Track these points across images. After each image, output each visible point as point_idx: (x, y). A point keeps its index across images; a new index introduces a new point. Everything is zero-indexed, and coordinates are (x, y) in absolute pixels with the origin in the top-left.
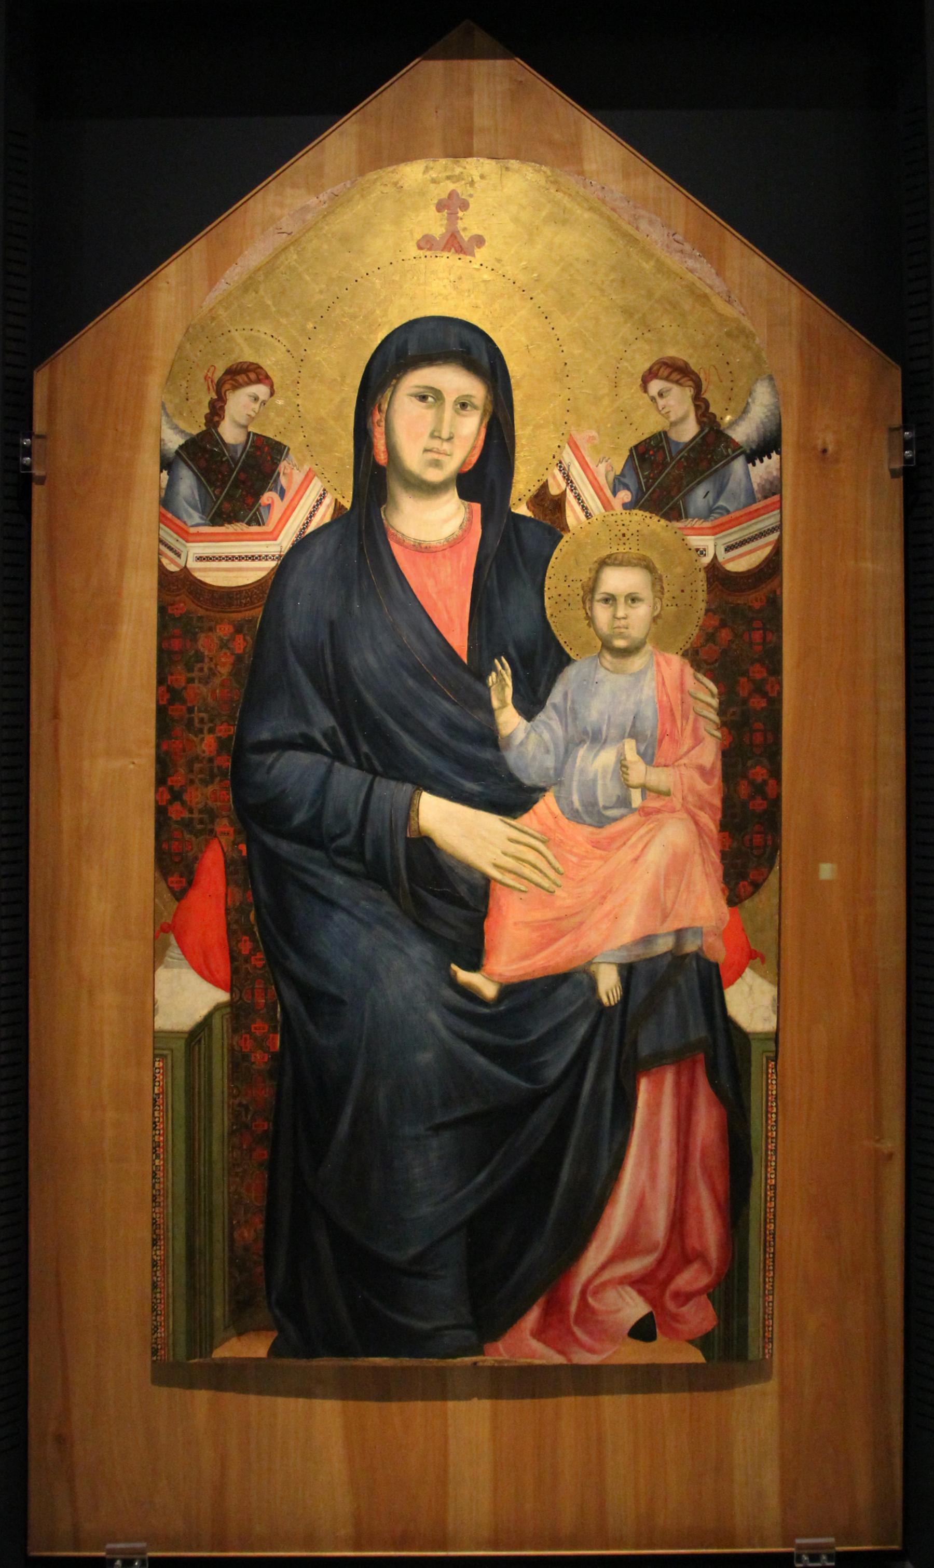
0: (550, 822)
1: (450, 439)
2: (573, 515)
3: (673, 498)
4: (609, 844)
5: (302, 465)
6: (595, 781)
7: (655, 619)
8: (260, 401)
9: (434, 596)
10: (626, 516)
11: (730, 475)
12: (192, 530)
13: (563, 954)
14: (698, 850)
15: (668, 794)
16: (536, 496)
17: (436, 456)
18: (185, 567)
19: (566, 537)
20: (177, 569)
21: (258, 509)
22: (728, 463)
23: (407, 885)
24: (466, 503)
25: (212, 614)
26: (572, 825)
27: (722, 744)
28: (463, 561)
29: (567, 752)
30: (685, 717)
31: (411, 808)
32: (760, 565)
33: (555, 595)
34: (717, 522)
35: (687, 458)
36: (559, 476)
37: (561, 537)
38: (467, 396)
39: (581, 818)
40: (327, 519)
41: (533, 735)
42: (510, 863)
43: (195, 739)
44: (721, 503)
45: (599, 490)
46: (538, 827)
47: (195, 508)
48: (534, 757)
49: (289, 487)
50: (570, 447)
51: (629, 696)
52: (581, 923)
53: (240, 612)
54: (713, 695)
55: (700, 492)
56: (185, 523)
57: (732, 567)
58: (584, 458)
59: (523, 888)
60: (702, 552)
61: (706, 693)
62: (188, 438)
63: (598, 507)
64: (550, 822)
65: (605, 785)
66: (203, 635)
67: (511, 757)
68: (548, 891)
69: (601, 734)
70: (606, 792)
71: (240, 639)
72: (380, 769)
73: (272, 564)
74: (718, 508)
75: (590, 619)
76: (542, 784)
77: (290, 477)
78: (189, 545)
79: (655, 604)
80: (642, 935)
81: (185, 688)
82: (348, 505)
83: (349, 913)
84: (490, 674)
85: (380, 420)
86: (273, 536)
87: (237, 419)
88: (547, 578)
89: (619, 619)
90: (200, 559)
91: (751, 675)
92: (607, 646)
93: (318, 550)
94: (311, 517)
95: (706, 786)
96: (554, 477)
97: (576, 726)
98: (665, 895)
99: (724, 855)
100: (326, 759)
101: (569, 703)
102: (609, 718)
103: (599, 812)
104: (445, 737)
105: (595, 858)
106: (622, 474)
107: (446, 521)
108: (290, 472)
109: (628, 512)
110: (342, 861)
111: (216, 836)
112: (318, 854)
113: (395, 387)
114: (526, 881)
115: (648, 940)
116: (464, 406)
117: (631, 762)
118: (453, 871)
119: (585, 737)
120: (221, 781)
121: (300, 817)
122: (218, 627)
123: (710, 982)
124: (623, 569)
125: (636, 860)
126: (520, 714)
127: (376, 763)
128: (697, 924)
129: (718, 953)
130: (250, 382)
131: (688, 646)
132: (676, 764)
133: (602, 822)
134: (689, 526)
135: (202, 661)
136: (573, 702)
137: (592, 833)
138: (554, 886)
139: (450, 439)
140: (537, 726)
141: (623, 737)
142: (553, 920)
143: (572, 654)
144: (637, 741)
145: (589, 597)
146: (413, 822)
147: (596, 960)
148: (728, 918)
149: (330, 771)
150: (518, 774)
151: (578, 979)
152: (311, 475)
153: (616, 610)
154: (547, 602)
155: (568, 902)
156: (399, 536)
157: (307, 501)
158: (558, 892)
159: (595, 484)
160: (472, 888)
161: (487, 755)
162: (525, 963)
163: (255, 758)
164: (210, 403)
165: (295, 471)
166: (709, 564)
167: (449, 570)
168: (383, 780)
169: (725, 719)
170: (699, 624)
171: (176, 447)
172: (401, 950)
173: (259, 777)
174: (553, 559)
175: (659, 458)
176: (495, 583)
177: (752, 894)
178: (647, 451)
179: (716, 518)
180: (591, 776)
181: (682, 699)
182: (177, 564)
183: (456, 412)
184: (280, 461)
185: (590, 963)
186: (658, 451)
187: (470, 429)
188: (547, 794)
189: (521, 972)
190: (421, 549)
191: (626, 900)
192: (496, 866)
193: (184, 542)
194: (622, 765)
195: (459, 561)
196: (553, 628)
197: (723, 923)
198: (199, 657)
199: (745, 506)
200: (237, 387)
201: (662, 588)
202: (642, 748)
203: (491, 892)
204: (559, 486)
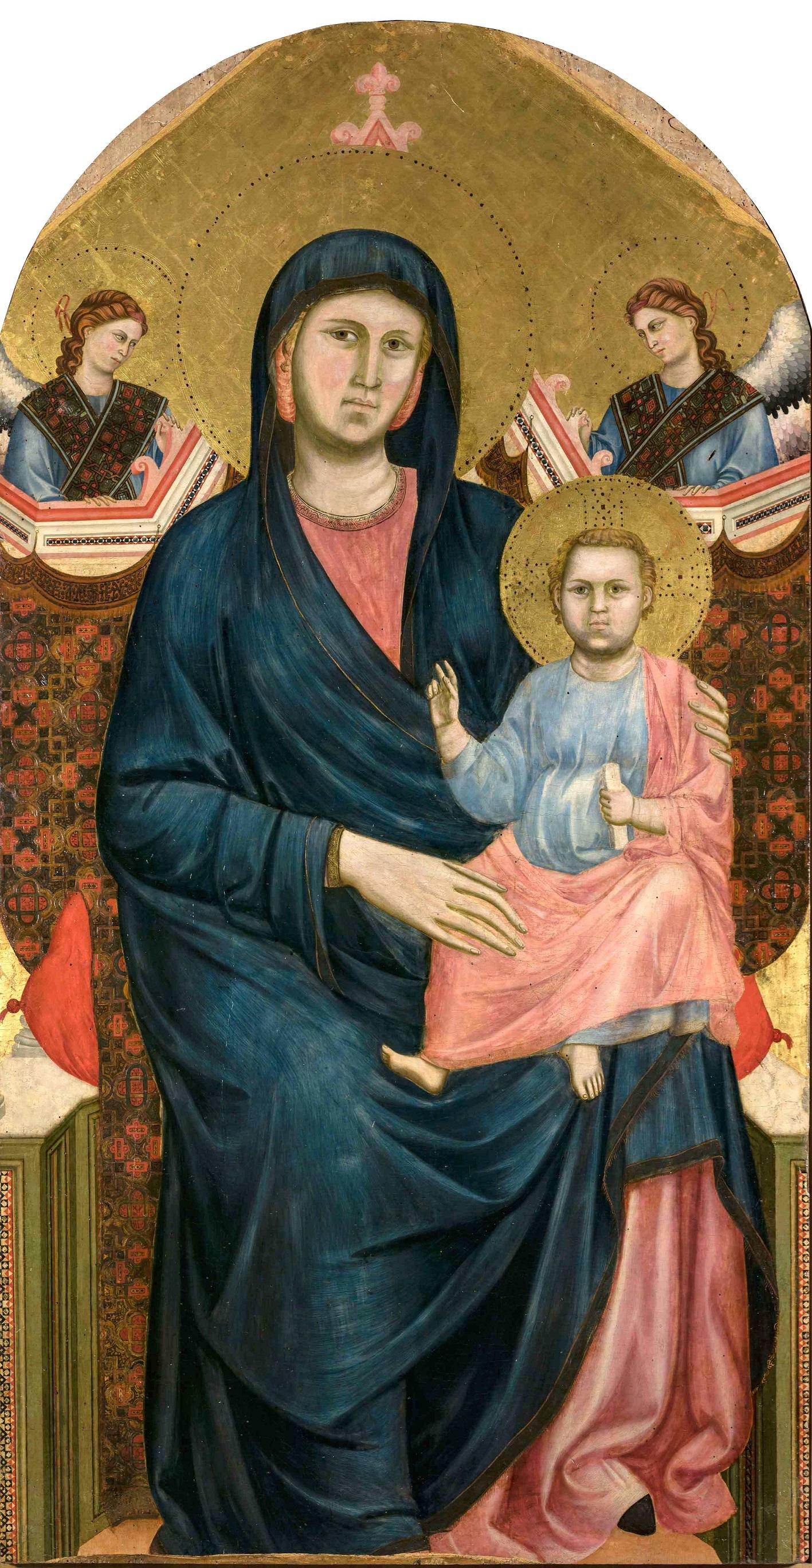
0: (508, 867)
1: (376, 387)
3: (669, 459)
4: (586, 895)
5: (185, 419)
6: (567, 815)
7: (645, 613)
8: (129, 341)
9: (357, 585)
11: (744, 429)
12: (42, 506)
13: (528, 1033)
14: (702, 903)
15: (662, 832)
16: (488, 458)
17: (358, 409)
18: (34, 552)
19: (527, 510)
21: (127, 479)
22: (741, 414)
23: (324, 947)
24: (398, 467)
25: (70, 612)
26: (537, 870)
27: (733, 770)
29: (530, 778)
30: (684, 735)
31: (329, 850)
32: (782, 544)
34: (726, 490)
35: (687, 409)
36: (519, 434)
37: (522, 509)
38: (398, 331)
39: (548, 861)
40: (218, 491)
41: (486, 758)
42: (458, 919)
43: (49, 768)
44: (731, 465)
45: (569, 449)
46: (493, 873)
47: (46, 479)
48: (488, 786)
49: (168, 450)
50: (533, 396)
51: (610, 710)
52: (552, 994)
53: (107, 608)
54: (721, 709)
55: (704, 450)
56: (32, 496)
57: (744, 546)
58: (550, 409)
59: (475, 950)
60: (706, 528)
61: (712, 706)
62: (35, 388)
63: (569, 472)
64: (508, 867)
65: (579, 820)
66: (58, 638)
67: (458, 787)
68: (506, 953)
69: (575, 758)
70: (581, 829)
71: (106, 641)
72: (289, 802)
73: (148, 547)
74: (725, 472)
75: (560, 614)
76: (498, 820)
77: (168, 437)
78: (37, 524)
79: (644, 593)
80: (630, 1010)
81: (34, 705)
82: (244, 472)
83: (251, 983)
84: (429, 682)
85: (285, 364)
86: (148, 512)
87: (100, 363)
88: (503, 561)
89: (597, 613)
90: (52, 542)
91: (771, 681)
92: (581, 647)
94: (196, 487)
95: (712, 823)
96: (512, 434)
97: (541, 748)
98: (659, 961)
99: (736, 910)
100: (219, 791)
101: (533, 719)
102: (585, 736)
103: (572, 854)
104: (371, 761)
105: (569, 913)
106: (601, 430)
107: (372, 491)
108: (169, 432)
109: (608, 477)
110: (239, 918)
111: (78, 890)
112: (209, 909)
113: (304, 320)
114: (477, 941)
115: (638, 1015)
116: (394, 344)
117: (614, 792)
118: (385, 929)
119: (553, 761)
120: (84, 820)
121: (187, 864)
122: (78, 628)
123: (720, 1071)
124: (602, 549)
125: (620, 915)
126: (469, 733)
127: (284, 795)
128: (702, 996)
129: (730, 1033)
130: (116, 317)
131: (689, 645)
132: (673, 794)
133: (575, 866)
134: (689, 494)
135: (57, 671)
136: (538, 718)
137: (564, 882)
138: (515, 948)
139: (376, 387)
140: (492, 748)
141: (604, 762)
142: (514, 989)
143: (536, 658)
144: (621, 766)
145: (559, 585)
146: (331, 868)
147: (571, 1041)
148: (742, 989)
149: (224, 806)
150: (466, 807)
151: (547, 1065)
152: (196, 434)
153: (592, 601)
154: (504, 594)
155: (533, 968)
156: (311, 510)
157: (193, 463)
158: (520, 955)
159: (566, 442)
160: (409, 950)
161: (428, 783)
162: (478, 1044)
163: (125, 791)
164: (63, 342)
165: (176, 430)
166: (715, 543)
167: (376, 554)
168: (294, 816)
169: (736, 738)
170: (703, 619)
171: (19, 400)
172: (319, 1029)
173: (133, 814)
174: (511, 538)
175: (650, 409)
176: (436, 568)
177: (776, 958)
178: (633, 400)
179: (724, 485)
180: (562, 809)
181: (680, 713)
182: (22, 550)
183: (384, 351)
185: (562, 1044)
186: (648, 400)
187: (402, 370)
188: (505, 831)
189: (473, 1056)
190: (339, 526)
191: (608, 965)
192: (440, 922)
193: (32, 522)
194: (602, 796)
196: (511, 624)
197: (735, 994)
198: (53, 666)
199: (763, 469)
201: (653, 573)
202: (628, 775)
203: (433, 954)
204: (519, 445)
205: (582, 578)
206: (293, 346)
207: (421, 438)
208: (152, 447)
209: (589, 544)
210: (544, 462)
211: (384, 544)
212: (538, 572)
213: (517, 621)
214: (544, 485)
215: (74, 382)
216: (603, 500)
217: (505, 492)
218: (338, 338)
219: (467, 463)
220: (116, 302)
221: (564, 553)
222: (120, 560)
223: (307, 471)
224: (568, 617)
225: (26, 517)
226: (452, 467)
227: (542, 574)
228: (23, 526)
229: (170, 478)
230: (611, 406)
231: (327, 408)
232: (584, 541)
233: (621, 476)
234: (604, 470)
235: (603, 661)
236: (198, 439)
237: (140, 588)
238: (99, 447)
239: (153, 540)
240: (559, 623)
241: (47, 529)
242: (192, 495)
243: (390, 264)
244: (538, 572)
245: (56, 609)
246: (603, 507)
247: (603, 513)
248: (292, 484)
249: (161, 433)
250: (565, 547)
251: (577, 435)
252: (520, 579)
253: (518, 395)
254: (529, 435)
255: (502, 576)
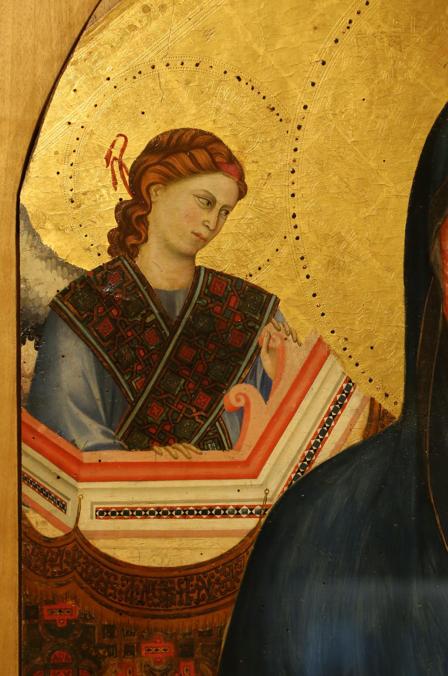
8: (218, 207)
12: (87, 458)
18: (76, 528)
20: (59, 533)
21: (218, 418)
25: (132, 621)
40: (356, 438)
47: (94, 415)
53: (188, 616)
56: (73, 443)
62: (76, 277)
77: (280, 356)
78: (81, 485)
86: (250, 469)
90: (104, 513)
93: (338, 497)
94: (323, 433)
122: (143, 646)
152: (322, 352)
164: (117, 209)
165: (290, 344)
171: (52, 295)
182: (58, 524)
184: (260, 323)
193: (72, 481)
200: (171, 178)
208: (254, 371)
215: (136, 269)
220: (198, 147)
222: (208, 542)
225: (63, 475)
228: (58, 488)
229: (283, 418)
236: (325, 358)
237: (238, 585)
238: (175, 368)
239: (258, 512)
241: (98, 494)
242: (316, 444)
245: (110, 617)
249: (268, 349)
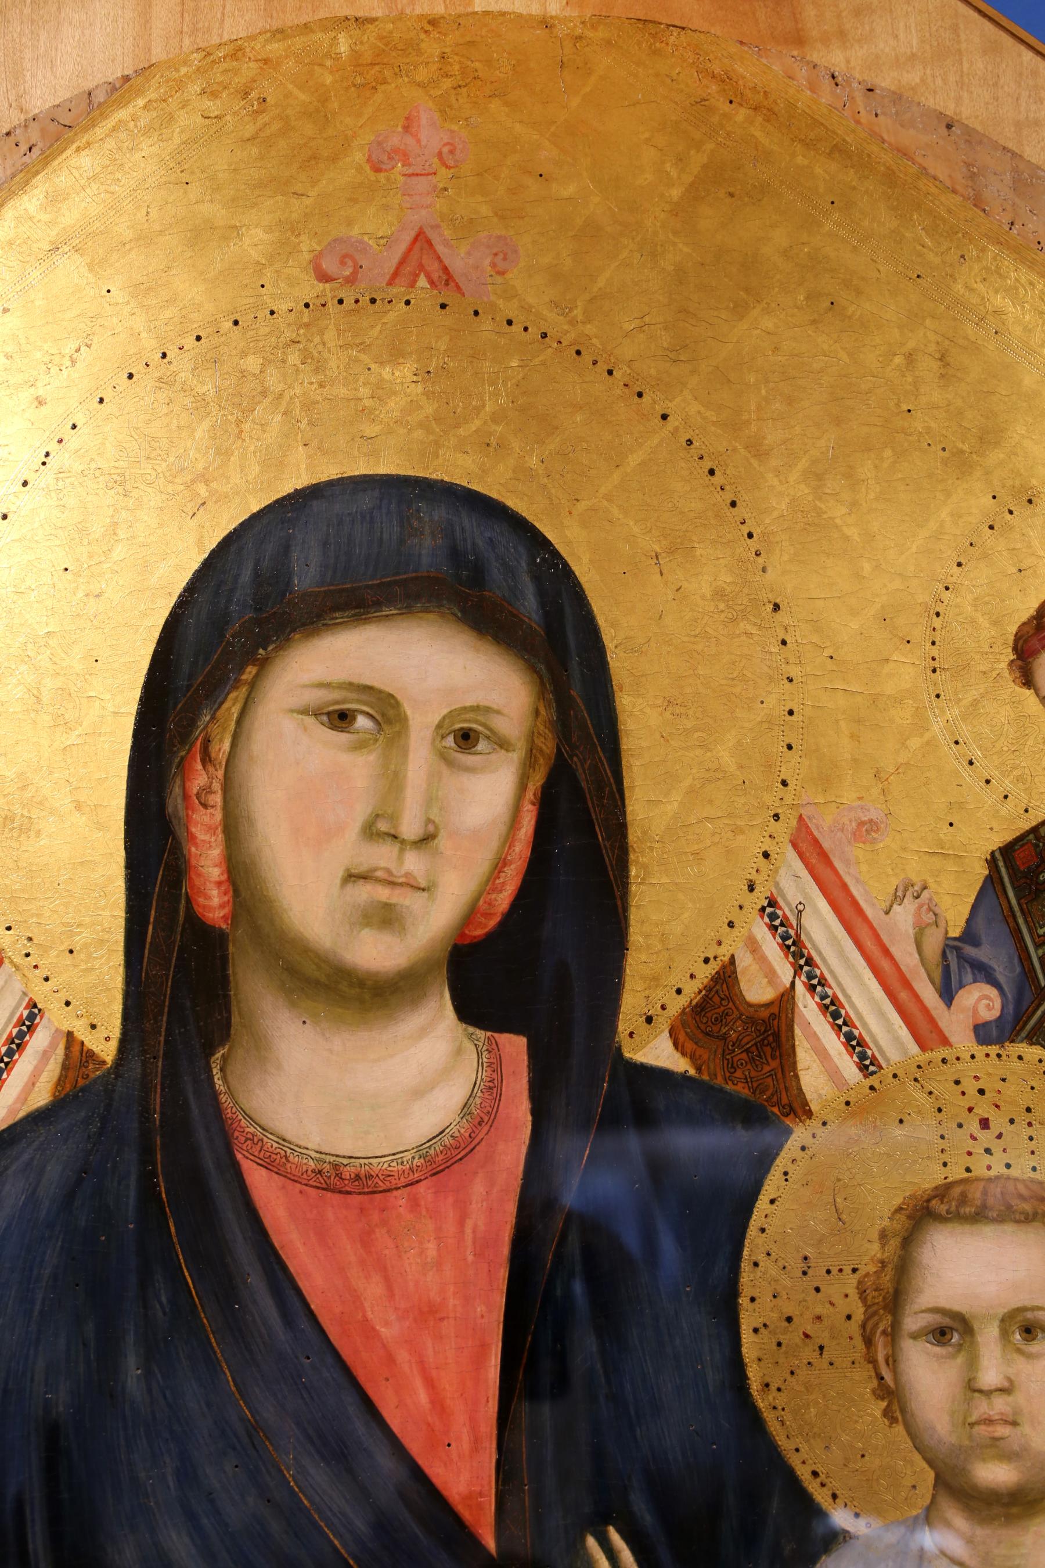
1: (426, 840)
2: (820, 1064)
10: (985, 1064)
17: (383, 893)
24: (481, 1034)
28: (477, 1219)
33: (773, 1317)
36: (771, 947)
38: (476, 709)
50: (801, 855)
58: (845, 886)
63: (897, 1039)
75: (893, 1398)
82: (106, 1049)
85: (208, 790)
88: (745, 1266)
89: (987, 1393)
92: (952, 1486)
96: (753, 946)
106: (969, 936)
107: (418, 1093)
113: (253, 685)
116: (466, 738)
145: (885, 1323)
153: (973, 1363)
156: (271, 1142)
159: (885, 965)
167: (431, 1249)
174: (762, 1204)
183: (443, 756)
187: (488, 802)
195: (461, 1223)
204: (771, 975)
205: (943, 1303)
206: (226, 746)
207: (538, 958)
209: (957, 1217)
210: (836, 1015)
211: (450, 1228)
212: (833, 1289)
213: (787, 1417)
214: (837, 1071)
216: (984, 1110)
217: (741, 1090)
218: (333, 727)
219: (649, 1020)
221: (894, 1243)
223: (261, 1046)
224: (913, 1405)
226: (614, 1030)
227: (844, 1296)
230: (989, 879)
231: (309, 891)
232: (942, 1209)
233: (1022, 1048)
234: (983, 1033)
235: (1010, 1520)
240: (893, 1420)
243: (455, 555)
244: (833, 1289)
246: (985, 1124)
247: (986, 1137)
248: (224, 1078)
250: (897, 1226)
251: (913, 949)
252: (789, 1310)
253: (766, 855)
254: (795, 948)
255: (743, 1301)
